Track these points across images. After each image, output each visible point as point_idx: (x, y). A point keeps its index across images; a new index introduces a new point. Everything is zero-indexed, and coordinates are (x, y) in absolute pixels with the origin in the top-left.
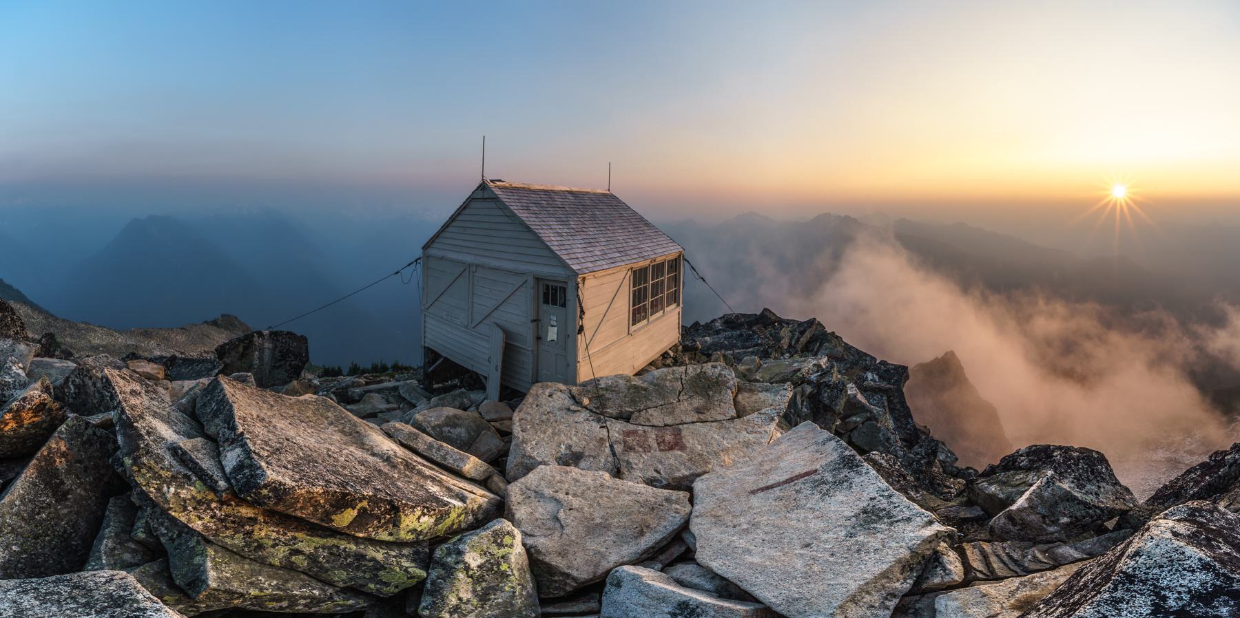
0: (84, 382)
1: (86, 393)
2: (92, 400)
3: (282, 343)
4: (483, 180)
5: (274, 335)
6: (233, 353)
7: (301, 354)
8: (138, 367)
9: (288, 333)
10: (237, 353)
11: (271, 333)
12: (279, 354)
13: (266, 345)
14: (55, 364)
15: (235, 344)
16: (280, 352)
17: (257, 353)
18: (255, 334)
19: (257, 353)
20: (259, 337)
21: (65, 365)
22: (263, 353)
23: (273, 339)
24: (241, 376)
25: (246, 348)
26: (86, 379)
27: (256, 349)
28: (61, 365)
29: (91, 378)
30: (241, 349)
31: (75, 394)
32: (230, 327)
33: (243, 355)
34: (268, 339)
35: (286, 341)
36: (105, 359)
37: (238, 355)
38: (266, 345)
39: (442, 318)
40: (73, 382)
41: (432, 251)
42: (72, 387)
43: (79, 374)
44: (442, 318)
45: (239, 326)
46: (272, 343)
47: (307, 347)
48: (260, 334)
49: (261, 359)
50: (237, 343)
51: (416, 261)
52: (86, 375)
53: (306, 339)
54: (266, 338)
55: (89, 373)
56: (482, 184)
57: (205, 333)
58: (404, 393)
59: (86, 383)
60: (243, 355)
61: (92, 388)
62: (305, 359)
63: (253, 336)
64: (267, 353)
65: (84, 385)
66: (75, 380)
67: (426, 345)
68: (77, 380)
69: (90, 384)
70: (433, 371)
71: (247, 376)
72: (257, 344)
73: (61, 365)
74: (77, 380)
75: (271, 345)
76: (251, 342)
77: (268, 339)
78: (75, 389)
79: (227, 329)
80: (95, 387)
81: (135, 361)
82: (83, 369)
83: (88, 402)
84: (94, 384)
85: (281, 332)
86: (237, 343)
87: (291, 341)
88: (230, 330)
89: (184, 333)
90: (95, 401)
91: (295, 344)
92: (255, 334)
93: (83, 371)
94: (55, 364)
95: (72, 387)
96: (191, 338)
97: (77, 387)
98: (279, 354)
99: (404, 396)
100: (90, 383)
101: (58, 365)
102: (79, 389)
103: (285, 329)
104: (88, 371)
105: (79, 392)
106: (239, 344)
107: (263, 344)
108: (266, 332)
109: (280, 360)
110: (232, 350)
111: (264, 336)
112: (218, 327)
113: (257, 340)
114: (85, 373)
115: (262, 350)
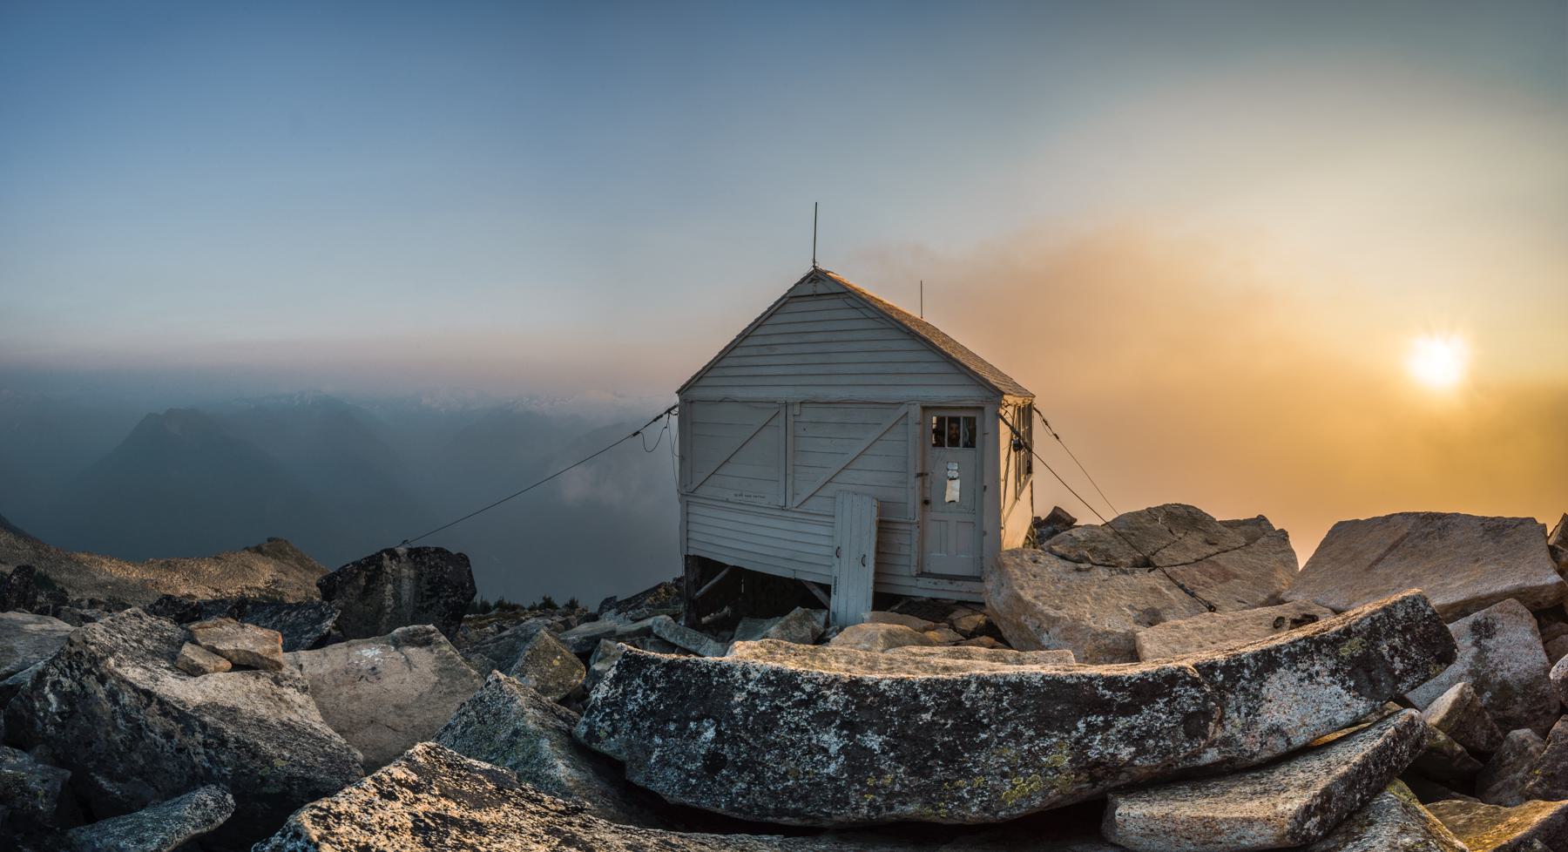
0: (83, 687)
1: (92, 717)
2: (108, 734)
3: (431, 567)
4: (814, 266)
5: (416, 554)
6: (349, 590)
7: (462, 585)
8: (220, 637)
9: (438, 550)
10: (354, 589)
11: (411, 552)
12: (429, 587)
13: (405, 571)
14: (26, 627)
15: (351, 572)
16: (429, 584)
17: (390, 586)
18: (384, 555)
19: (390, 586)
20: (391, 559)
21: (47, 626)
22: (400, 586)
23: (414, 561)
24: (416, 633)
25: (370, 580)
26: (90, 682)
27: (388, 581)
28: (40, 627)
29: (102, 679)
30: (362, 582)
31: (60, 714)
32: (279, 554)
33: (366, 592)
34: (407, 562)
35: (436, 564)
36: (135, 622)
37: (358, 592)
38: (405, 571)
39: (727, 501)
40: (54, 684)
41: (697, 393)
42: (51, 697)
43: (70, 667)
44: (727, 501)
45: (290, 553)
46: (415, 568)
47: (470, 571)
48: (393, 554)
49: (397, 596)
50: (355, 571)
51: (669, 411)
52: (89, 672)
53: (466, 559)
54: (403, 559)
55: (96, 665)
56: (811, 273)
57: (247, 563)
58: (671, 636)
59: (91, 691)
60: (366, 592)
61: (108, 706)
62: (470, 592)
63: (382, 558)
64: (407, 586)
65: (86, 695)
66: (59, 682)
67: (691, 553)
68: (66, 682)
69: (102, 696)
70: (702, 597)
71: (428, 632)
72: (390, 571)
73: (40, 627)
74: (66, 682)
75: (412, 571)
76: (380, 568)
77: (407, 562)
78: (60, 704)
79: (275, 557)
80: (116, 702)
81: (208, 623)
82: (80, 654)
83: (97, 738)
84: (113, 696)
85: (424, 548)
86: (355, 571)
87: (444, 563)
88: (279, 559)
89: (219, 564)
90: (117, 738)
91: (451, 567)
92: (384, 555)
93: (79, 660)
94: (26, 627)
95: (51, 697)
96: (228, 570)
97: (64, 697)
98: (429, 587)
99: (672, 640)
100: (101, 692)
101: (32, 627)
102: (71, 704)
103: (431, 543)
104: (95, 660)
105: (72, 713)
106: (359, 573)
107: (400, 572)
108: (402, 550)
109: (428, 597)
110: (348, 583)
111: (398, 556)
112: (263, 555)
113: (389, 565)
114: (86, 666)
115: (397, 581)
